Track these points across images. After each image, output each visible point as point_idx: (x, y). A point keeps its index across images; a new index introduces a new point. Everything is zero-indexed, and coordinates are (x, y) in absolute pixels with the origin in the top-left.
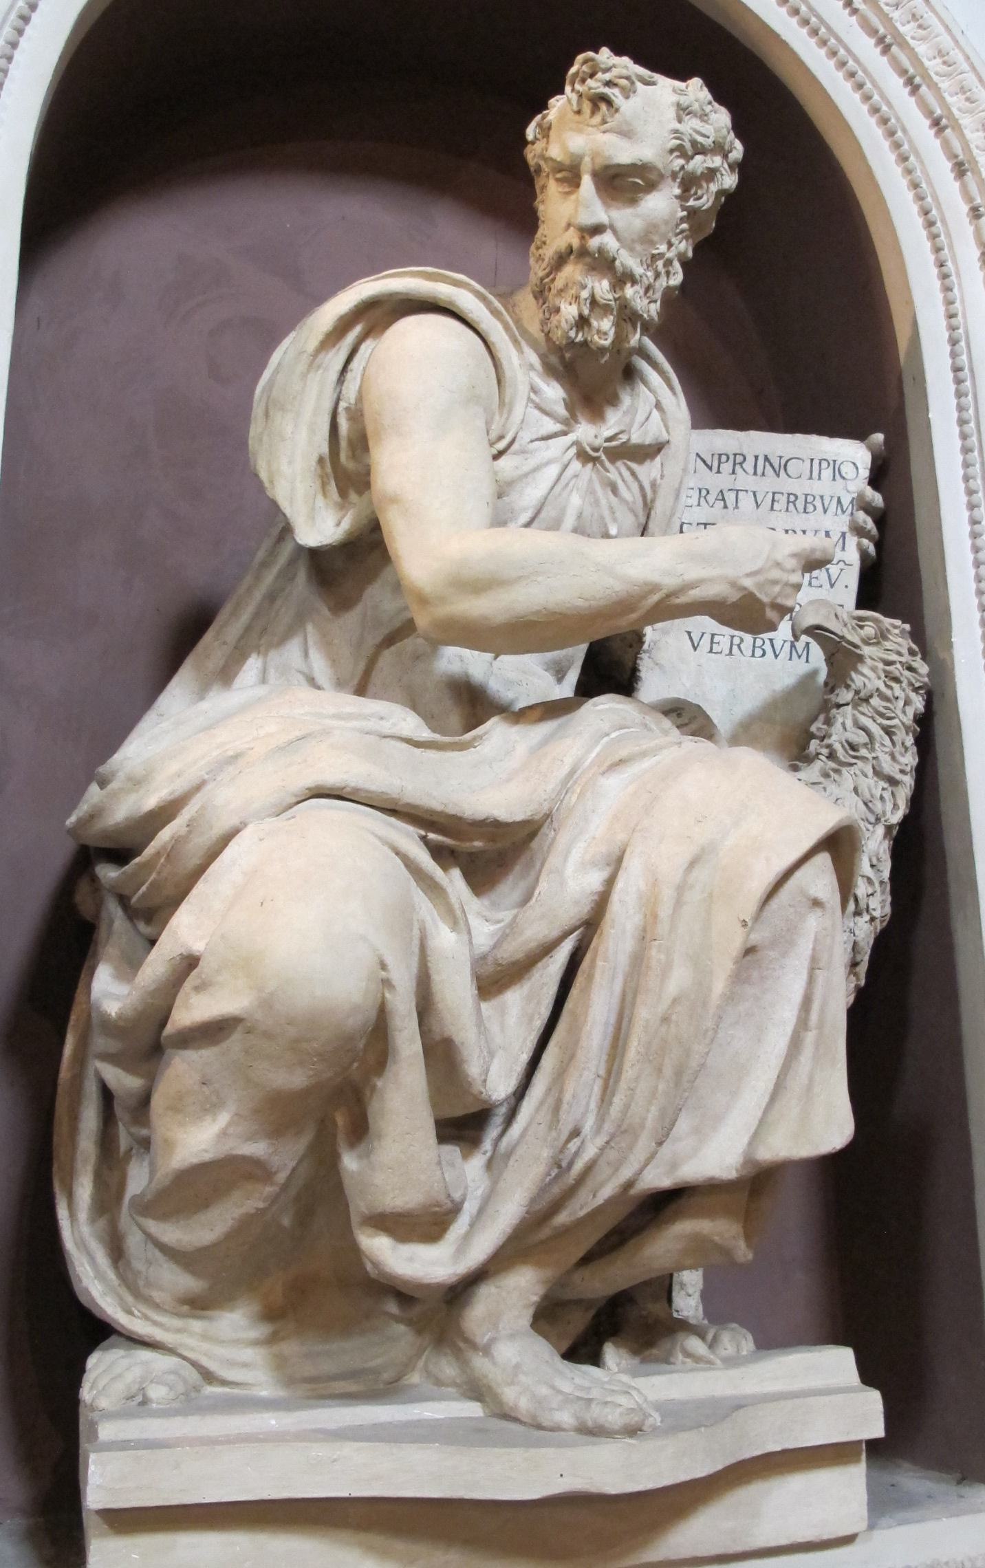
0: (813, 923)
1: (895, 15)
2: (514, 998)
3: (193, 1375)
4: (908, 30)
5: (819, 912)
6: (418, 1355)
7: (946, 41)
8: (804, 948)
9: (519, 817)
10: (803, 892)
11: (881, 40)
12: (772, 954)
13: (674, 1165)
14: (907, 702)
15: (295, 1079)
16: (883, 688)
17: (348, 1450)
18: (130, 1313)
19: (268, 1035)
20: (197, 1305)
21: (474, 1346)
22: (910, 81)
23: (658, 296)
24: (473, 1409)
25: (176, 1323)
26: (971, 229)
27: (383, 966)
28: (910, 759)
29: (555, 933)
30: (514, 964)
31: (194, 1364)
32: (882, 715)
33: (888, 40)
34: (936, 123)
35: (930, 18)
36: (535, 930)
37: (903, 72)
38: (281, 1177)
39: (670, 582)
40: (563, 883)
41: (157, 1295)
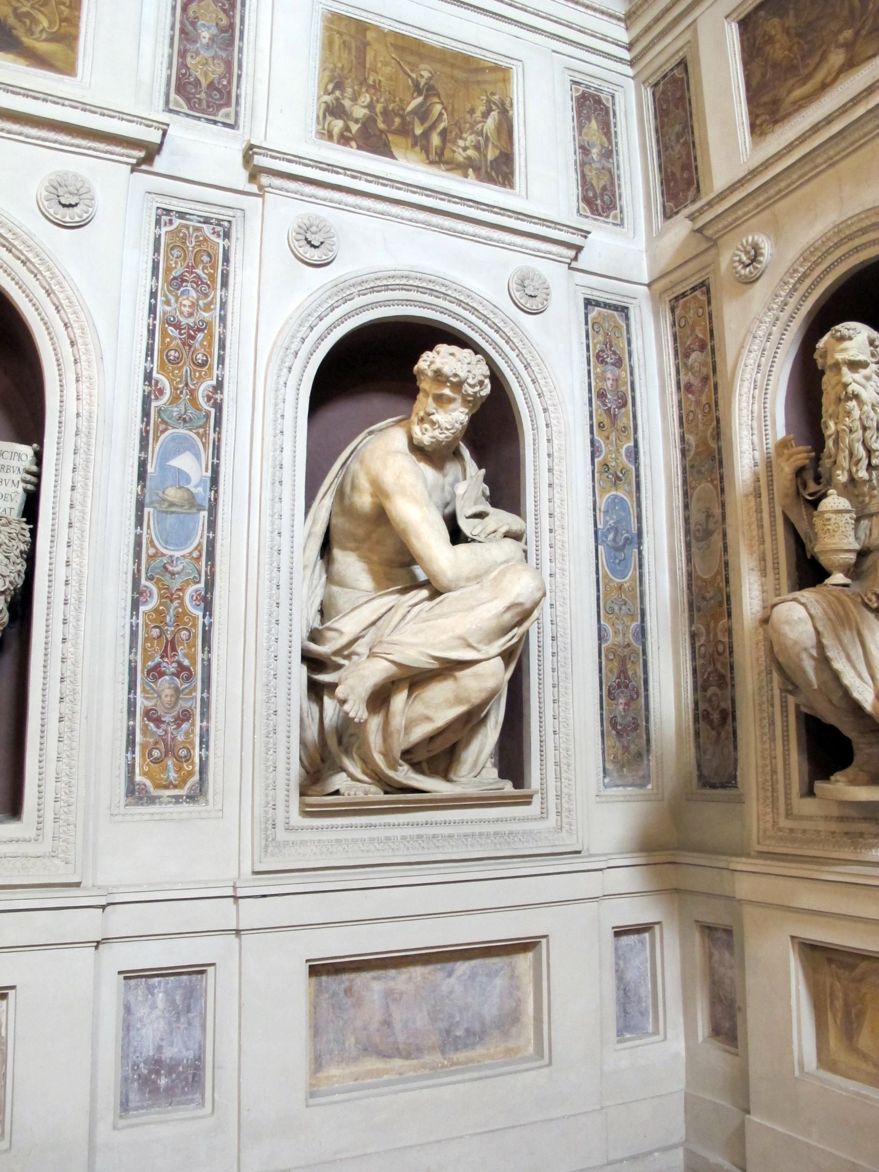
1: (52, 282)
4: (56, 288)
7: (70, 293)
11: (47, 291)
16: (7, 541)
22: (57, 308)
28: (22, 567)
34: (65, 325)
35: (65, 284)
37: (54, 304)
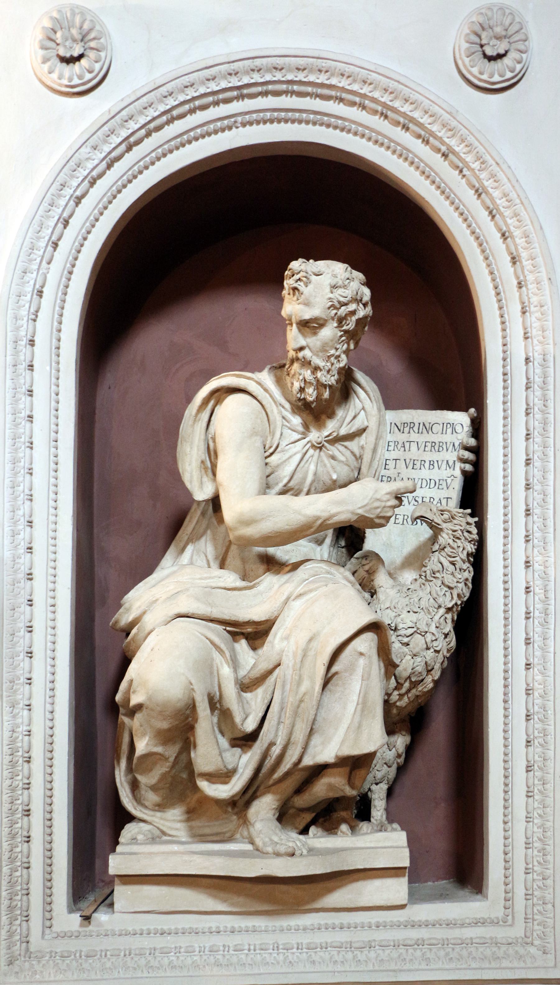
0: (362, 661)
2: (260, 691)
3: (158, 833)
5: (363, 658)
6: (238, 827)
8: (359, 671)
9: (263, 619)
10: (356, 651)
12: (347, 674)
13: (314, 757)
14: (464, 549)
15: (165, 725)
17: (195, 857)
18: (135, 809)
19: (152, 710)
20: (161, 807)
21: (251, 824)
23: (335, 372)
24: (249, 847)
25: (151, 813)
26: (517, 294)
27: (191, 684)
29: (271, 666)
30: (257, 678)
31: (158, 828)
32: (450, 556)
33: (480, 191)
36: (264, 666)
38: (172, 759)
39: (325, 515)
40: (273, 647)
41: (147, 803)
